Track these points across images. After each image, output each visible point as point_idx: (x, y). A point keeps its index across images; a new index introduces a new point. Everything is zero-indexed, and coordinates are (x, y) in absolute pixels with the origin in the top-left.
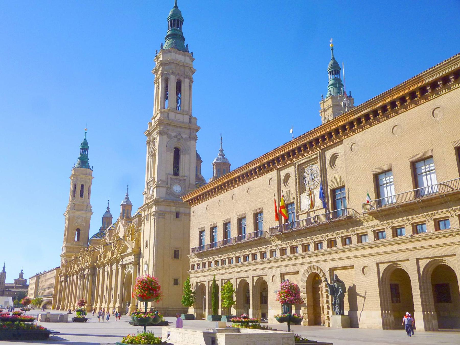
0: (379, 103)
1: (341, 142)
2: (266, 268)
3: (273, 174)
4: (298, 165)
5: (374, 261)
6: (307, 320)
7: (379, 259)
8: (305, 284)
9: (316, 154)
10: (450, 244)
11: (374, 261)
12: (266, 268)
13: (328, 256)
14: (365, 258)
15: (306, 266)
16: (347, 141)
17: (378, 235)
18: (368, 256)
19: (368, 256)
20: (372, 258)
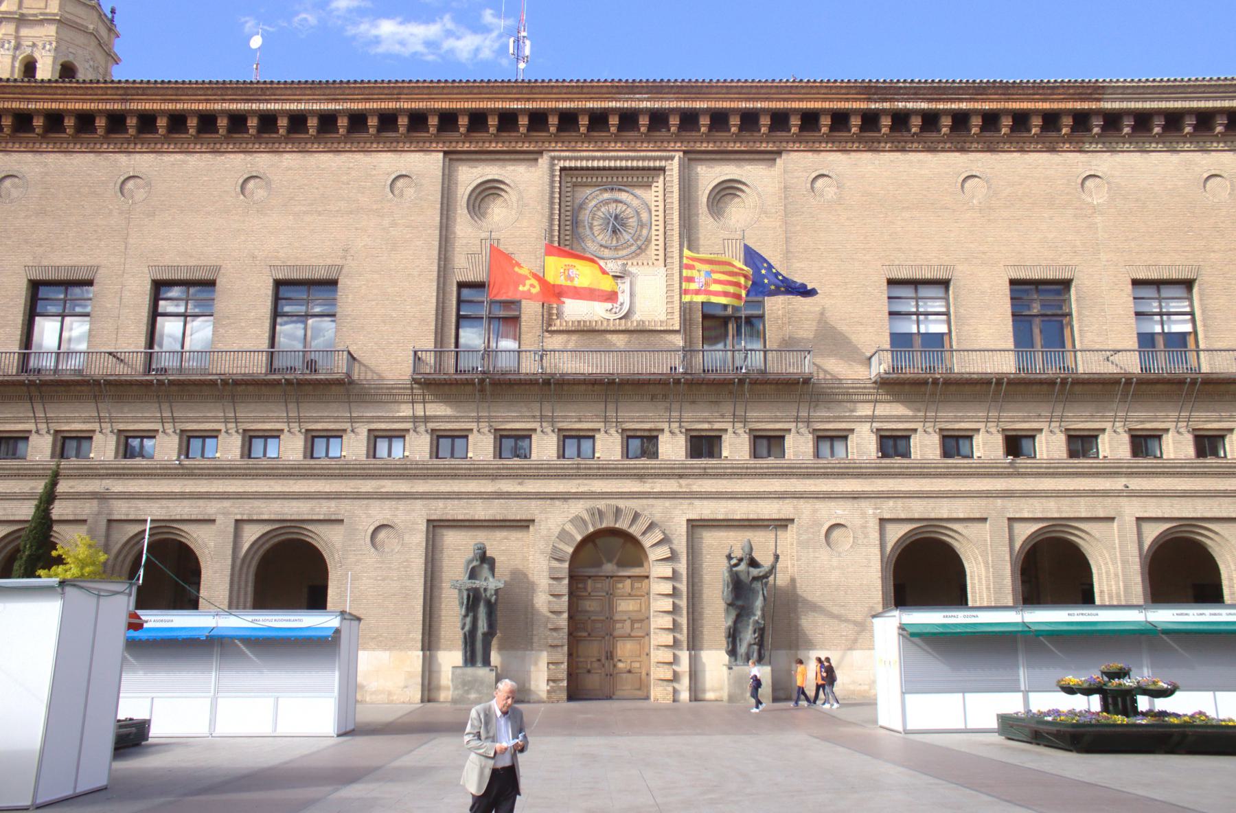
0: (961, 100)
1: (770, 157)
2: (338, 496)
3: (424, 164)
4: (563, 169)
5: (871, 512)
6: (565, 684)
7: (890, 509)
8: (566, 565)
9: (667, 159)
10: (1105, 494)
11: (871, 512)
12: (338, 496)
13: (683, 482)
14: (841, 502)
15: (578, 508)
16: (799, 164)
17: (893, 444)
18: (855, 496)
19: (855, 496)
20: (864, 504)
